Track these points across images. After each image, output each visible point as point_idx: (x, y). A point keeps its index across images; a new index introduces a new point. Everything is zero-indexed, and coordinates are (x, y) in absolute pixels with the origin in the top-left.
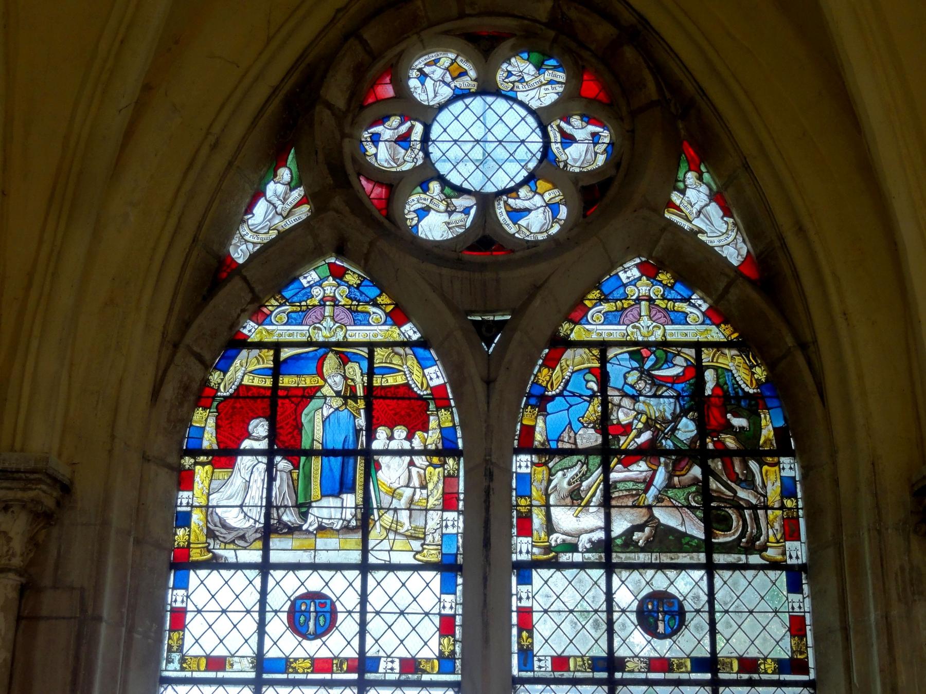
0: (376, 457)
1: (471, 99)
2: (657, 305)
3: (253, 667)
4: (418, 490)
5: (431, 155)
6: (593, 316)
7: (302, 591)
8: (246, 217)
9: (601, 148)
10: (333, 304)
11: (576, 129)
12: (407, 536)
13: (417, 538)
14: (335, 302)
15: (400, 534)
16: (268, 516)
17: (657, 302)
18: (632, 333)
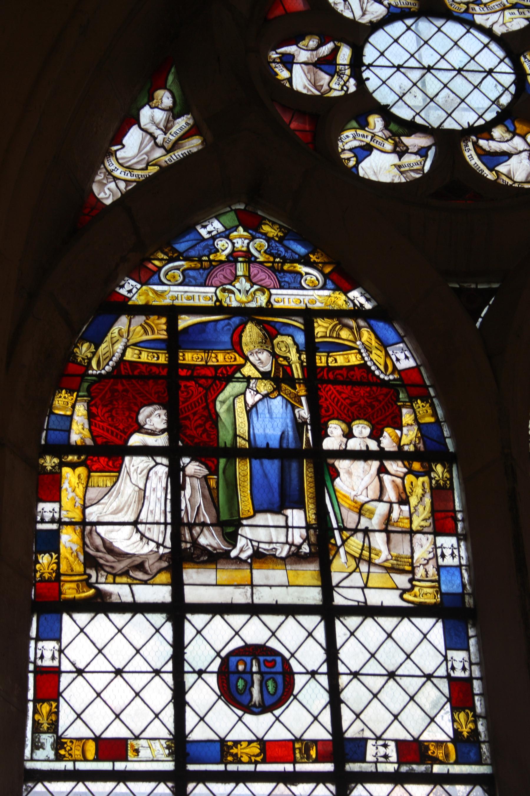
0: (330, 461)
3: (169, 755)
4: (396, 506)
5: (367, 83)
7: (237, 643)
8: (114, 148)
12: (386, 568)
13: (402, 572)
15: (376, 565)
16: (176, 537)
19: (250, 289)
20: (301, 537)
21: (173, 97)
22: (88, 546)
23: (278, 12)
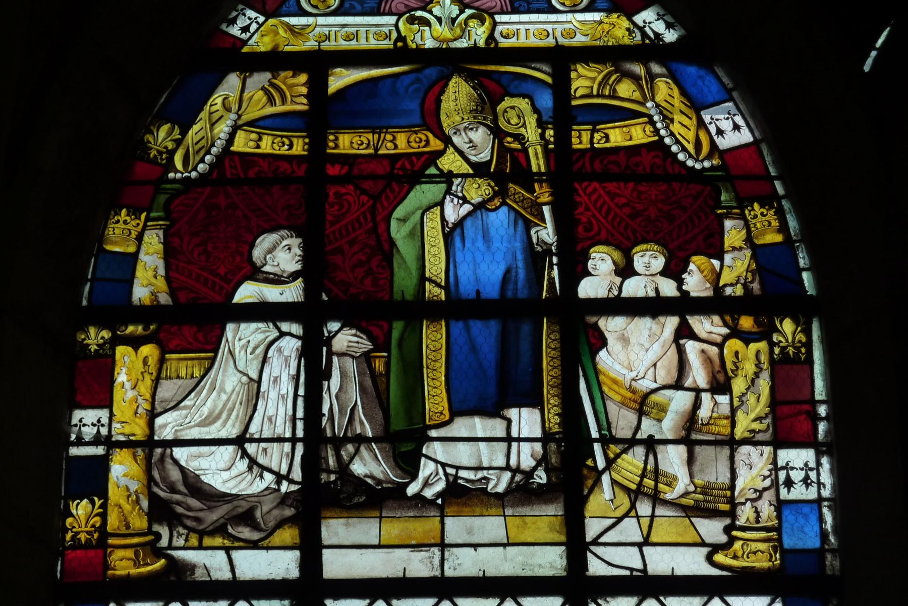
0: (592, 319)
4: (706, 397)
12: (684, 508)
13: (712, 514)
15: (666, 503)
16: (312, 464)
19: (458, 16)
20: (532, 456)
22: (157, 485)
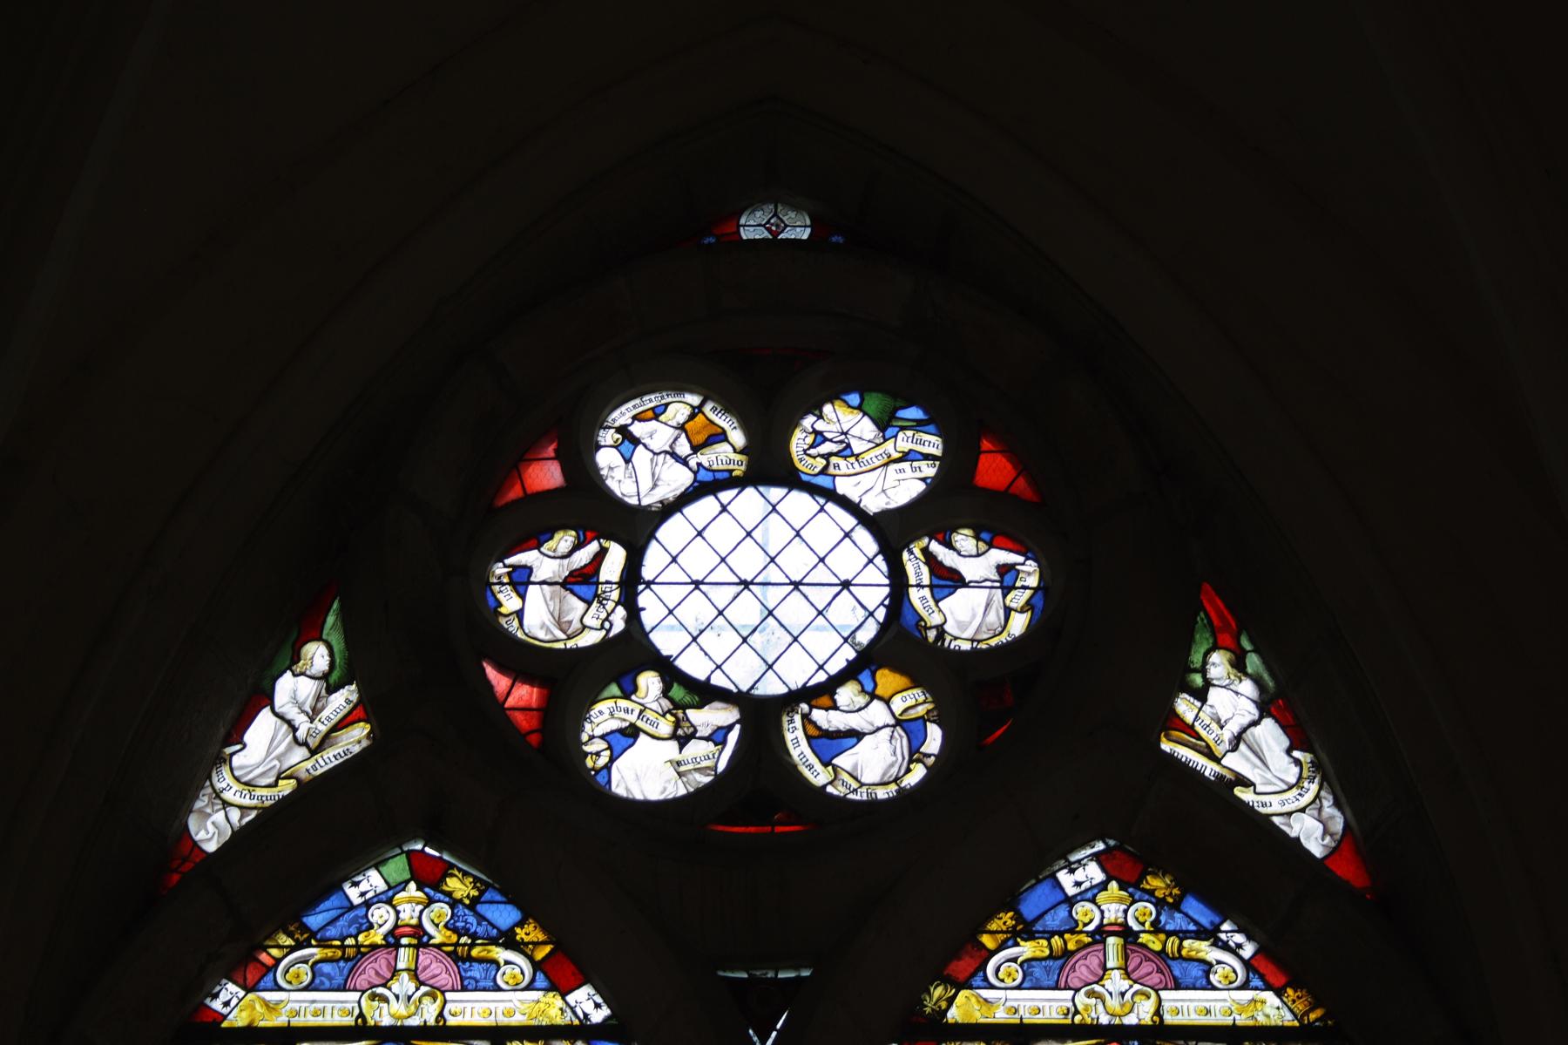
1: (732, 493)
2: (1144, 946)
6: (998, 970)
8: (229, 750)
9: (1018, 598)
10: (414, 941)
11: (964, 556)
14: (420, 938)
17: (1144, 938)
18: (1087, 1007)
19: (414, 993)
21: (331, 654)
23: (514, 493)
